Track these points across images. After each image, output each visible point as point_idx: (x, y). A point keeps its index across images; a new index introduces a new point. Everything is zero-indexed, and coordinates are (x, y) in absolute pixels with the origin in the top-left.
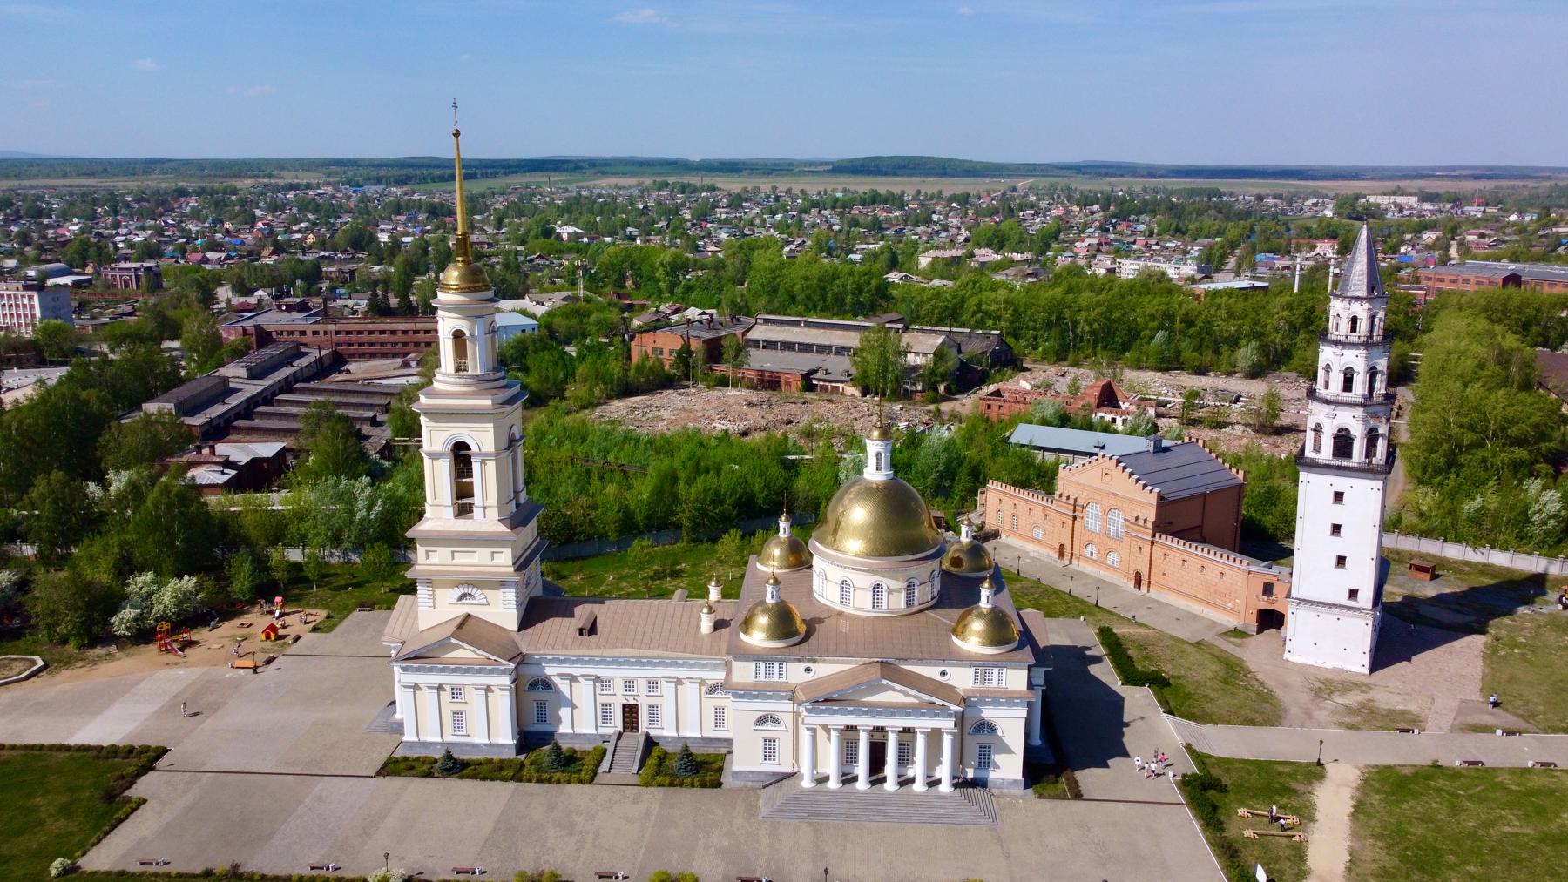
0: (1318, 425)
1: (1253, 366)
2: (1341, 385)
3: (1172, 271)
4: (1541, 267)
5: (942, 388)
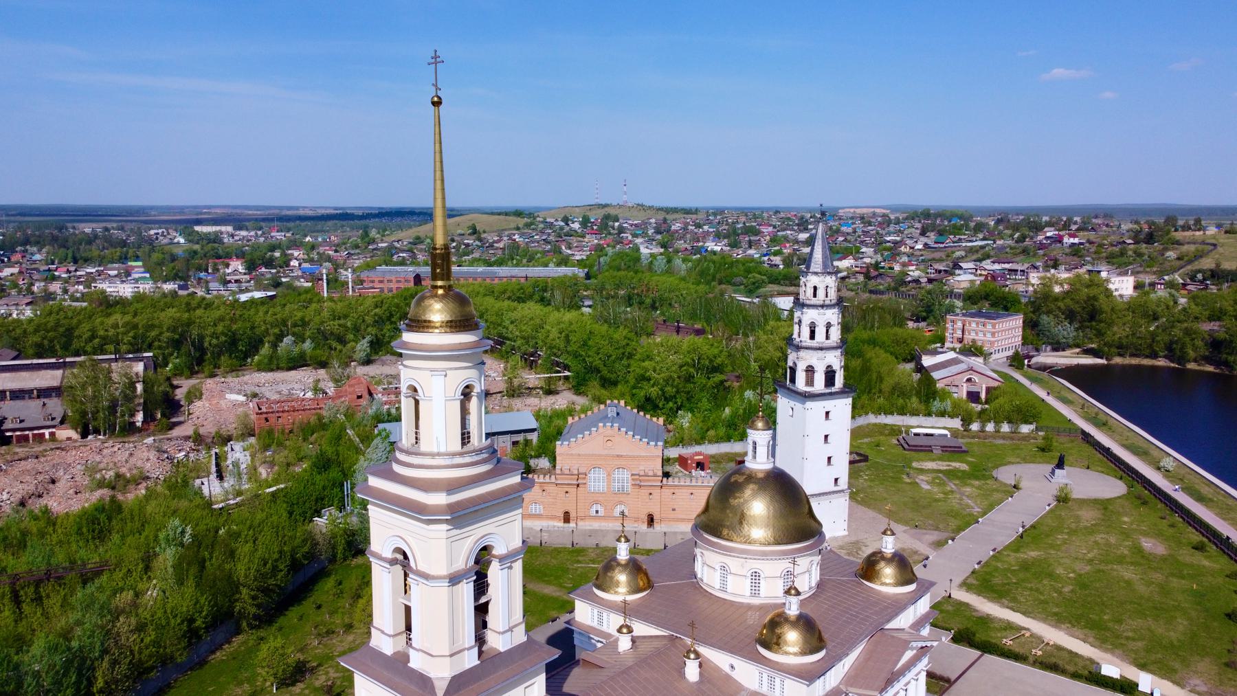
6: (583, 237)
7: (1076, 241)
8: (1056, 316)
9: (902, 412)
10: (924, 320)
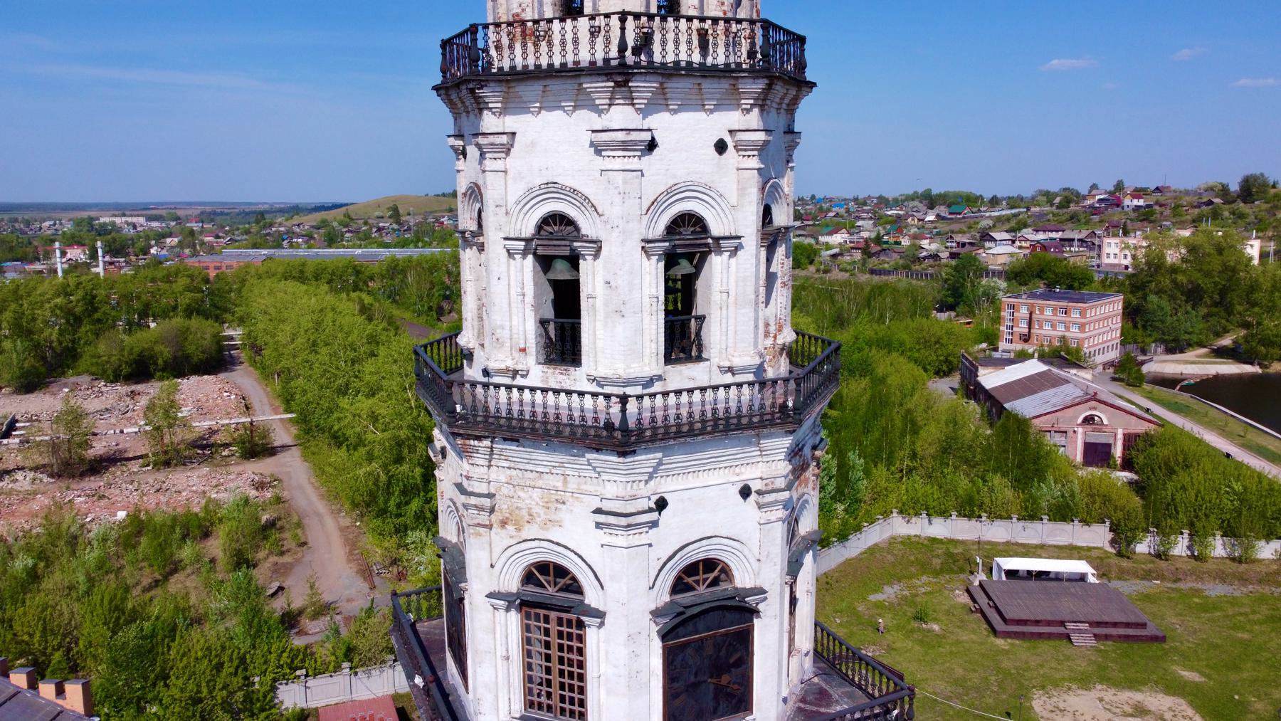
1: (25, 374)
7: (1141, 202)
8: (1172, 298)
9: (969, 509)
10: (951, 308)
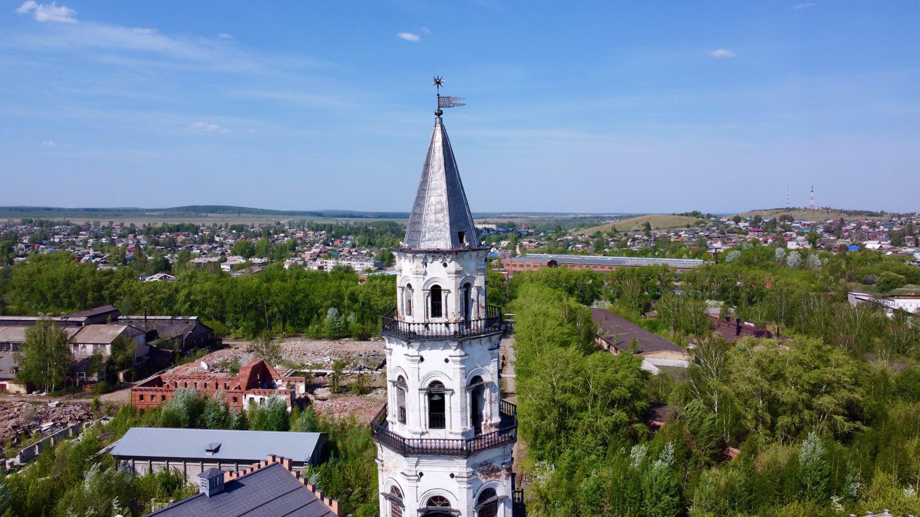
0: (395, 489)
2: (424, 416)
3: (357, 266)
4: (564, 256)
5: (121, 376)
6: (746, 234)
